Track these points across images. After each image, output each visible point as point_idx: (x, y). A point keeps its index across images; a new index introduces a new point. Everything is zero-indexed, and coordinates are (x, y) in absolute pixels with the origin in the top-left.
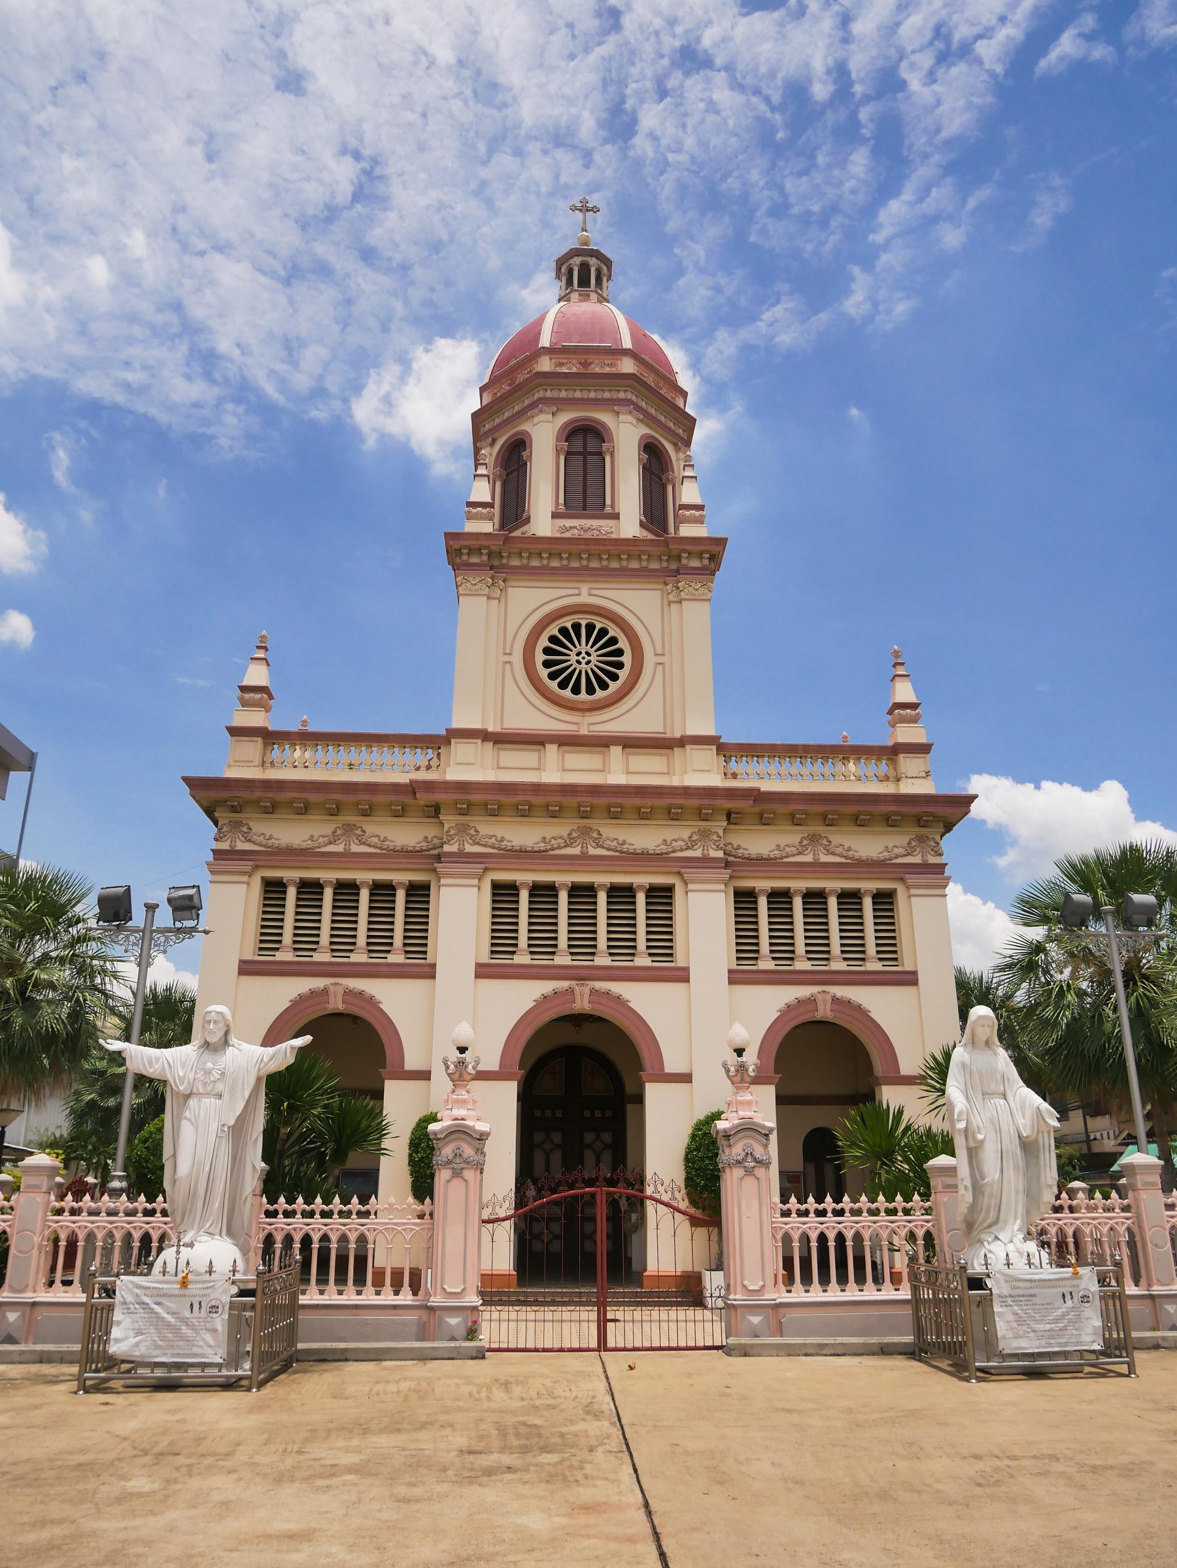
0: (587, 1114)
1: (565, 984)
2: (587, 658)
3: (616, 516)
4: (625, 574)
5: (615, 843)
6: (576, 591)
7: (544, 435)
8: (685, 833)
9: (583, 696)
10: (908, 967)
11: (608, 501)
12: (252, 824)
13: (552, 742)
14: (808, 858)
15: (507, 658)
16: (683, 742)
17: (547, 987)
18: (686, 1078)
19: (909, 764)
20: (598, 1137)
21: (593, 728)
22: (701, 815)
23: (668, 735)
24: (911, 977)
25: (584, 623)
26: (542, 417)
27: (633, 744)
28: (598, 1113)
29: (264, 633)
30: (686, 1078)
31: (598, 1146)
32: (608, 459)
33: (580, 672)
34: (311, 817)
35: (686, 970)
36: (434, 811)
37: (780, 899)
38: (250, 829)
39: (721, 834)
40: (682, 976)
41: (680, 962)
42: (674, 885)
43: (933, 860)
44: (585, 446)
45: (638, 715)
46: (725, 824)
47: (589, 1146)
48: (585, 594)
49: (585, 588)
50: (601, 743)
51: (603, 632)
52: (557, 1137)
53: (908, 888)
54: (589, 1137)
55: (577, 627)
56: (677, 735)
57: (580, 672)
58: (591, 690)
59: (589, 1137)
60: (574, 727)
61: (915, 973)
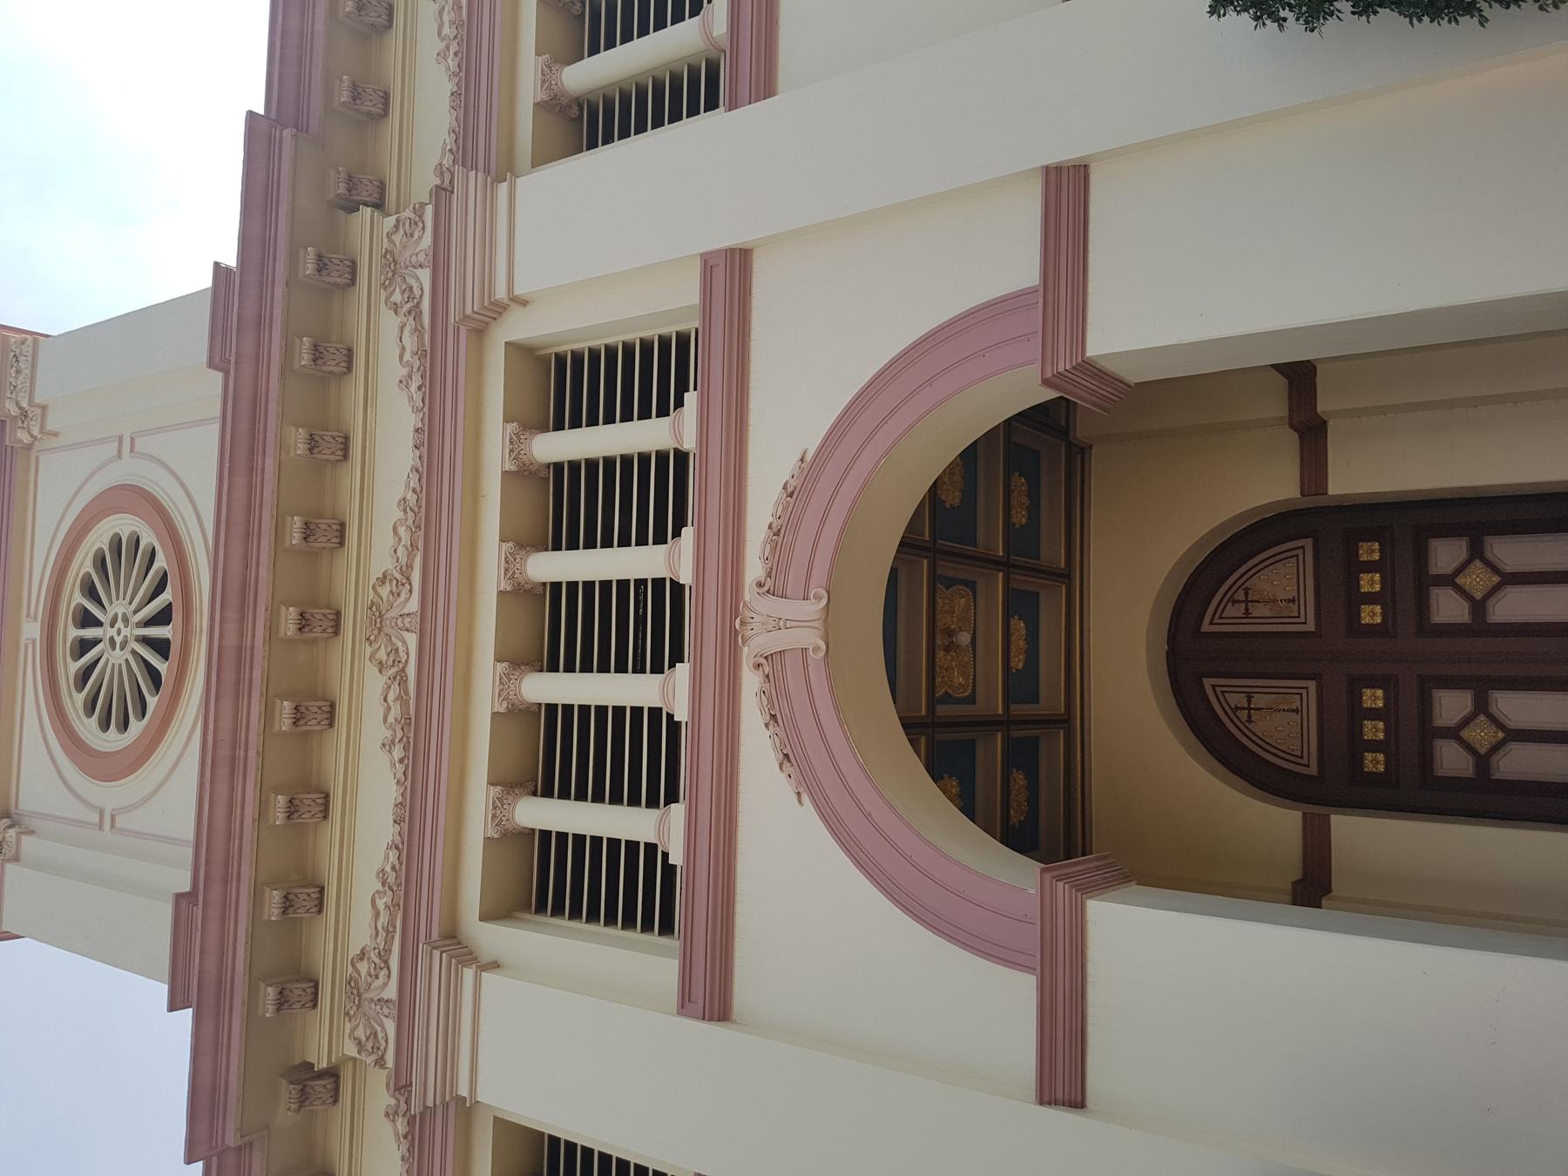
0: (1371, 615)
1: (751, 683)
5: (402, 530)
17: (757, 746)
18: (1066, 194)
20: (1449, 581)
28: (1370, 583)
30: (1066, 194)
31: (1477, 580)
35: (708, 263)
36: (319, 1084)
39: (390, 222)
40: (730, 274)
42: (517, 350)
47: (1479, 607)
52: (1451, 706)
54: (1448, 608)
59: (1448, 608)
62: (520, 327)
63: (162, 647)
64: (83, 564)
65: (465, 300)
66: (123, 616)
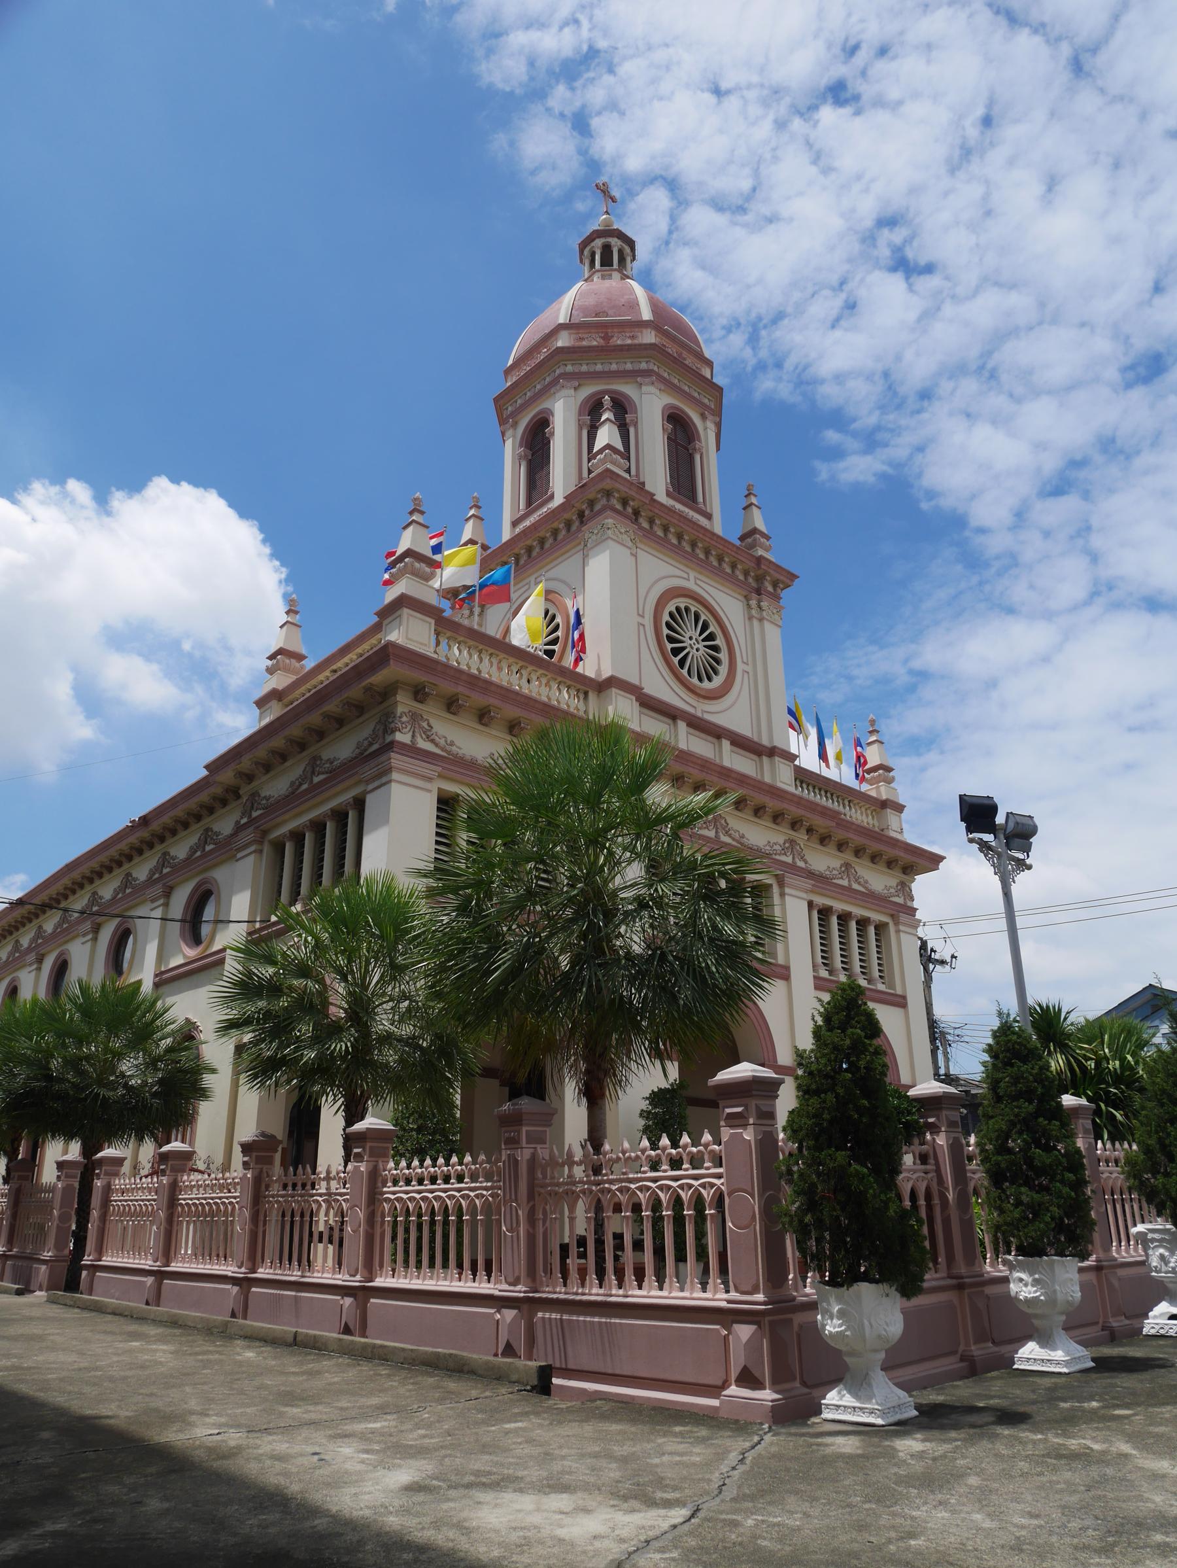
2: (697, 646)
3: (709, 517)
4: (717, 573)
6: (685, 576)
7: (652, 406)
8: (782, 842)
9: (695, 680)
10: (899, 991)
11: (700, 499)
12: (432, 721)
13: (683, 719)
14: (845, 883)
15: (640, 620)
16: (773, 752)
19: (891, 816)
21: (707, 717)
22: (795, 825)
23: (756, 739)
24: (901, 1000)
25: (693, 609)
26: (651, 389)
27: (741, 743)
29: (418, 495)
32: (697, 458)
33: (688, 654)
34: (494, 732)
37: (824, 913)
38: (429, 725)
41: (781, 960)
42: (771, 885)
43: (909, 904)
44: (681, 434)
45: (732, 714)
46: (806, 837)
48: (694, 581)
49: (692, 574)
50: (716, 733)
51: (705, 626)
53: (897, 923)
55: (687, 609)
56: (765, 742)
57: (688, 654)
58: (700, 679)
60: (692, 710)
61: (904, 997)
62: (776, 890)
63: (676, 652)
64: (723, 656)
65: (789, 879)
66: (696, 649)
